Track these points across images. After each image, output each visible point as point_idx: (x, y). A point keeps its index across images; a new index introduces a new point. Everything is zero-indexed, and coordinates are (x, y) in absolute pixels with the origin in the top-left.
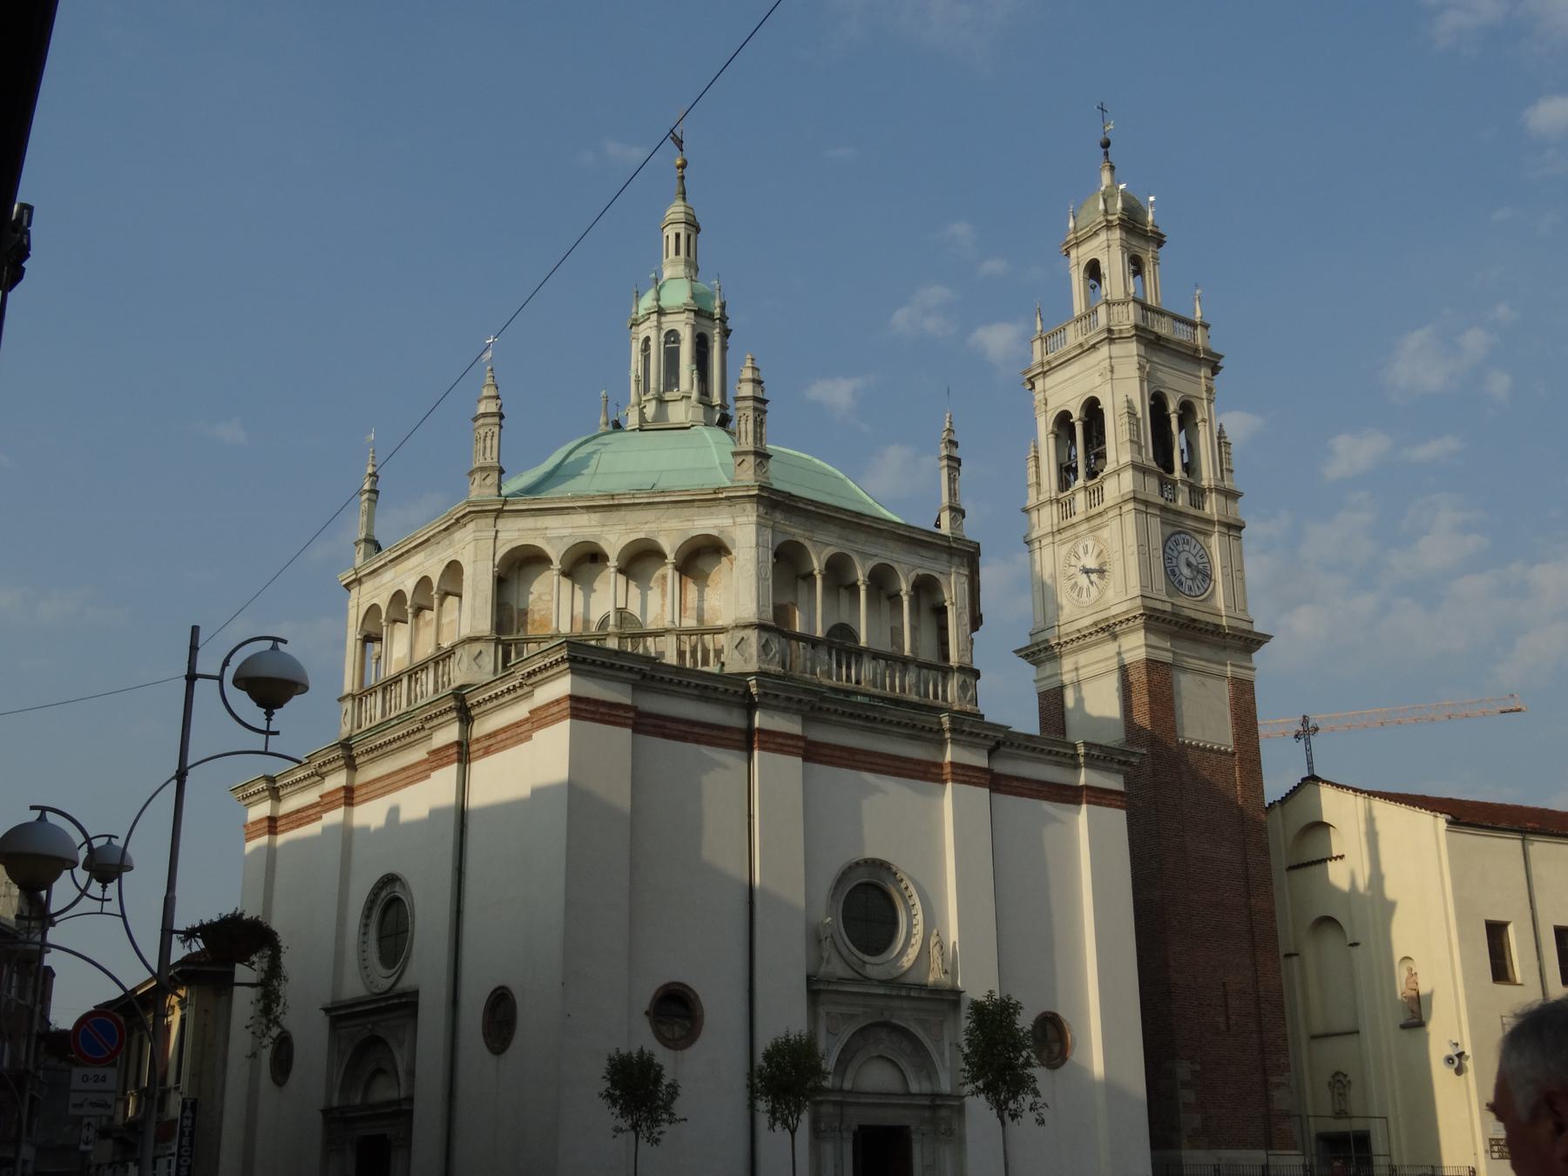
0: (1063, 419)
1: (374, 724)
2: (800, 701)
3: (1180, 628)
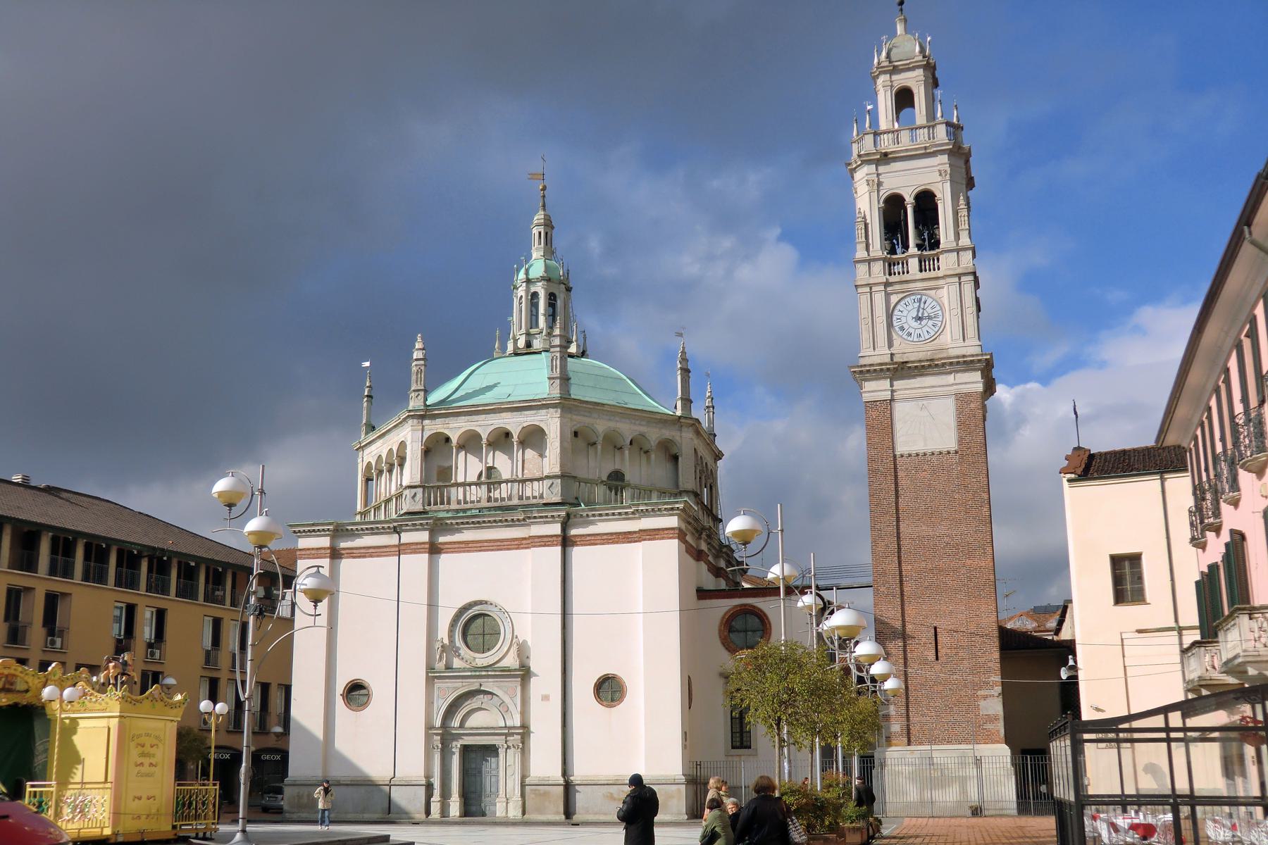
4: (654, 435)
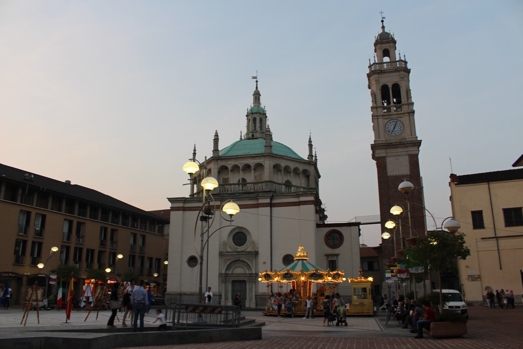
2: (217, 198)
4: (301, 167)
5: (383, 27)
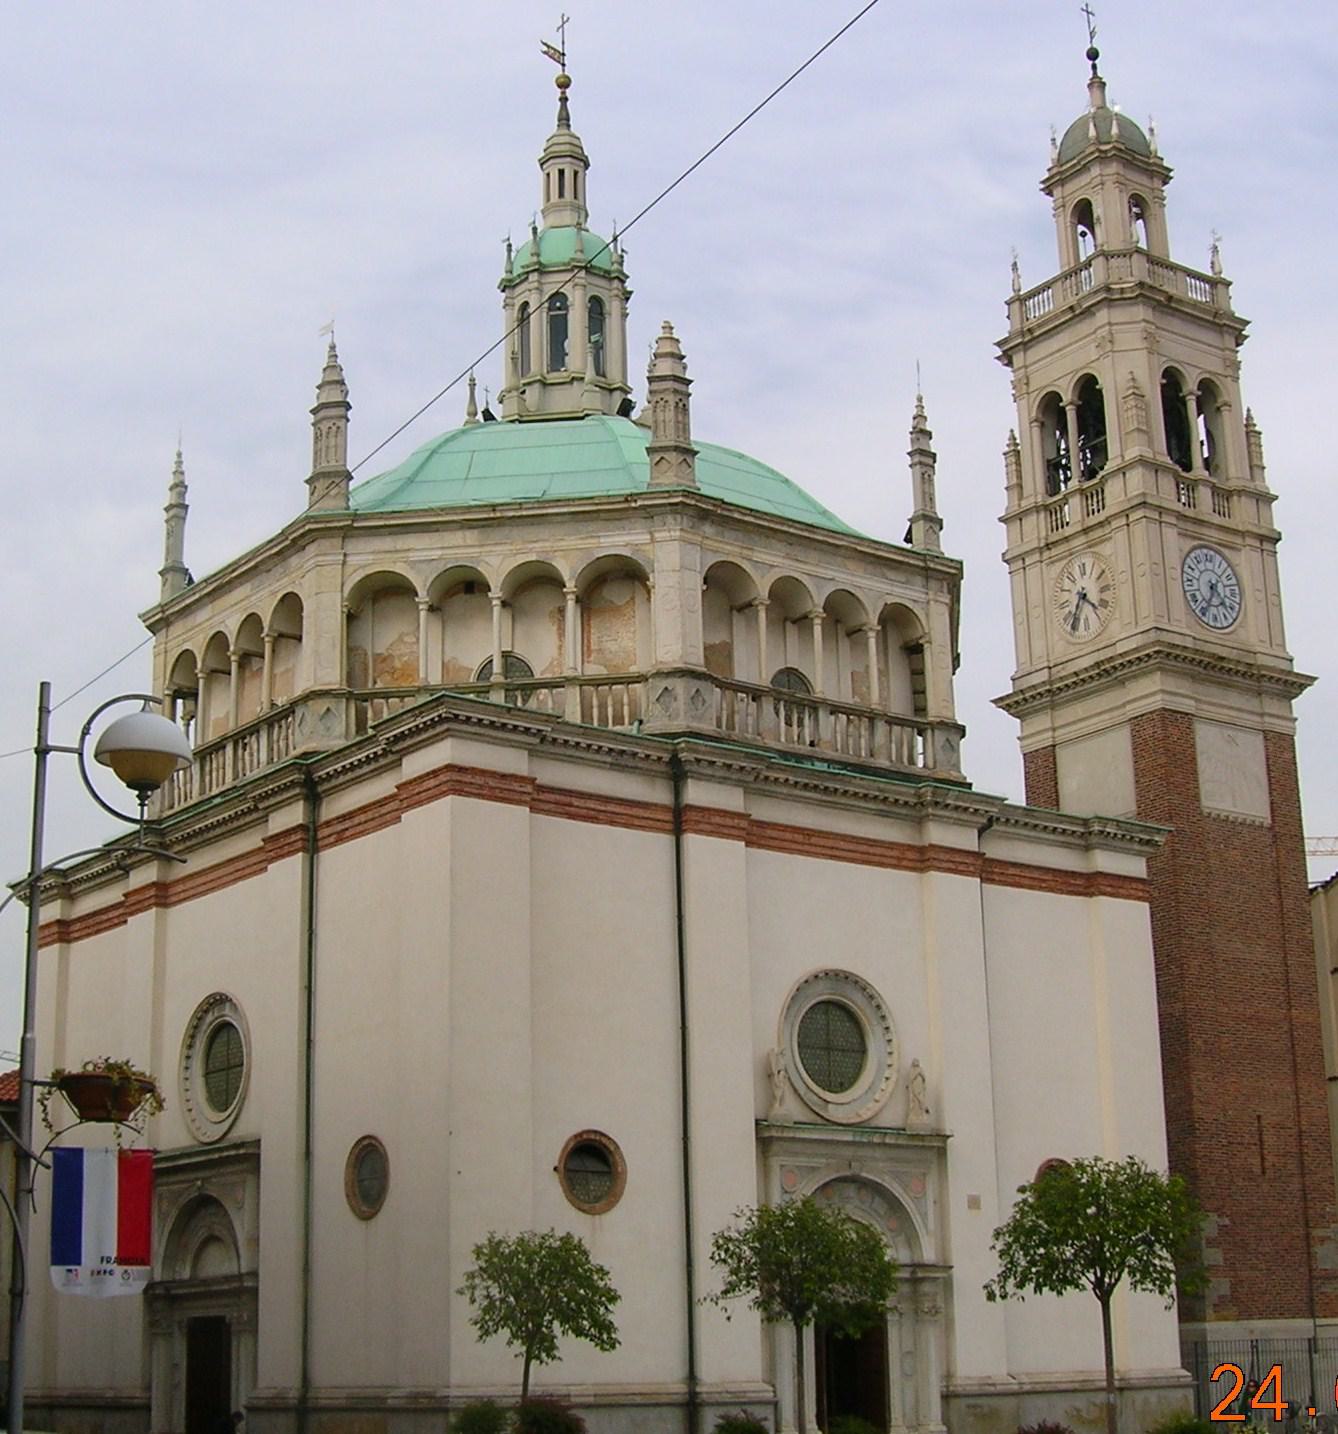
0: (1051, 406)
1: (191, 802)
2: (742, 768)
3: (1205, 668)
5: (1097, 84)
